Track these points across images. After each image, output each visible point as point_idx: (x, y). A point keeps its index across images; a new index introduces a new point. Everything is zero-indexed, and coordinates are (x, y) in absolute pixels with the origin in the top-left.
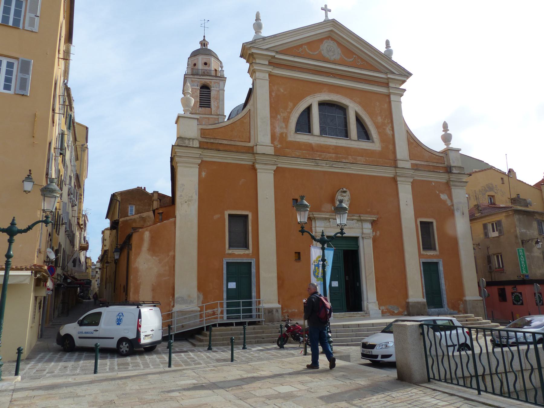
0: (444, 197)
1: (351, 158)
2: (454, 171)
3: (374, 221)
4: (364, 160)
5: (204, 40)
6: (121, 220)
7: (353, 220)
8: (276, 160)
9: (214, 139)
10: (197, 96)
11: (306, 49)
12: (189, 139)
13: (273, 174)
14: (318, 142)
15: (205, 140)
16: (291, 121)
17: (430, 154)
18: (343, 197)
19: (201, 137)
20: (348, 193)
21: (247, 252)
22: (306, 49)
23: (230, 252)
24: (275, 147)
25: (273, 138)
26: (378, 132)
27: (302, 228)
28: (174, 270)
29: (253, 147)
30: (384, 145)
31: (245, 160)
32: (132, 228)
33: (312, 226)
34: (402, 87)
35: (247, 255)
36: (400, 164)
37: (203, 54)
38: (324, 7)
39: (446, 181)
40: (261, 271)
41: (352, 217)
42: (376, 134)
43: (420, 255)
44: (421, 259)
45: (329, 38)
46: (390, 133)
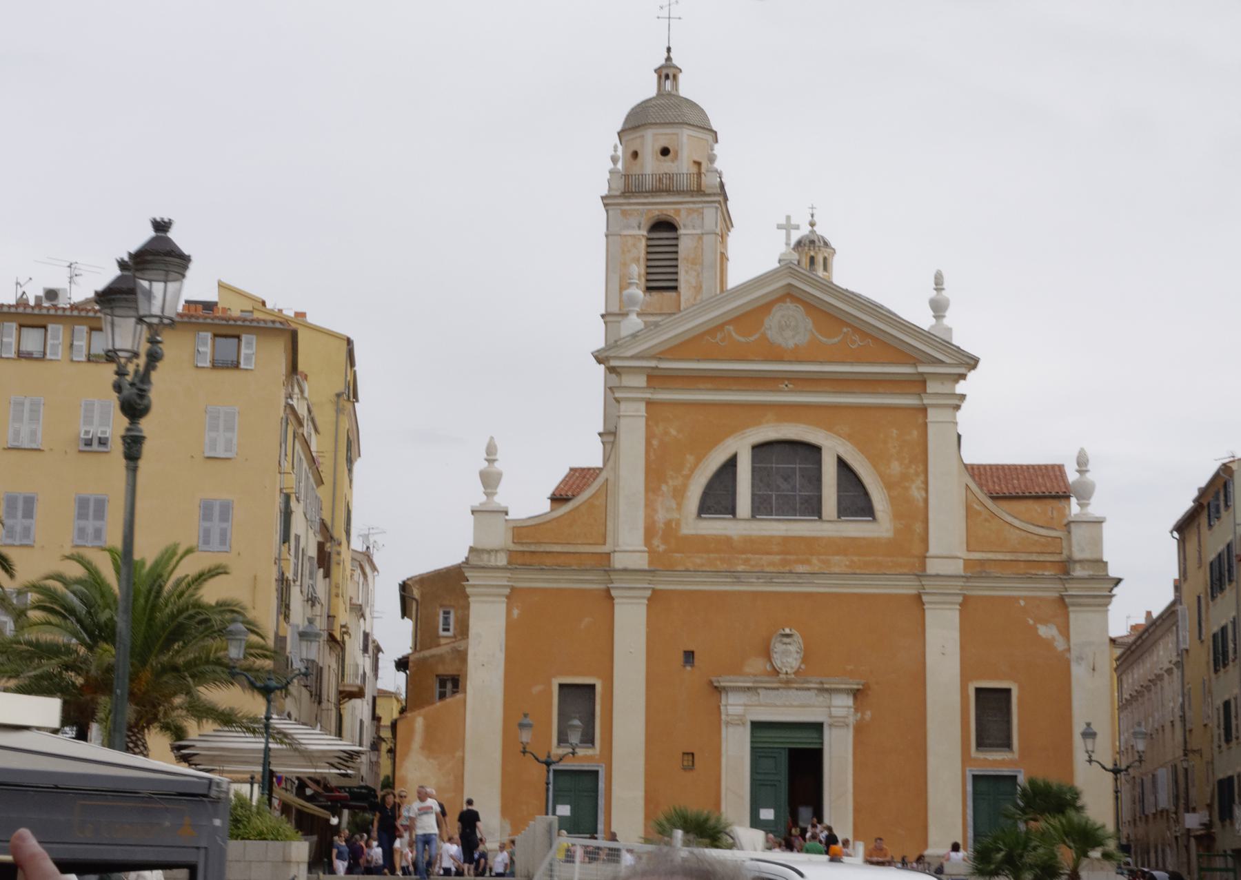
0: (1045, 631)
2: (1078, 572)
3: (858, 690)
4: (847, 563)
5: (669, 59)
6: (411, 658)
7: (809, 689)
8: (651, 578)
10: (639, 258)
12: (489, 552)
14: (745, 533)
16: (689, 494)
17: (1024, 534)
18: (784, 646)
19: (514, 542)
20: (798, 637)
24: (652, 552)
25: (649, 533)
26: (889, 496)
27: (524, 748)
28: (463, 782)
29: (609, 554)
31: (592, 583)
32: (437, 676)
33: (720, 702)
34: (960, 388)
35: (591, 758)
36: (933, 567)
37: (656, 124)
38: (783, 221)
39: (1057, 595)
40: (614, 787)
41: (803, 683)
43: (966, 759)
44: (968, 769)
45: (781, 299)
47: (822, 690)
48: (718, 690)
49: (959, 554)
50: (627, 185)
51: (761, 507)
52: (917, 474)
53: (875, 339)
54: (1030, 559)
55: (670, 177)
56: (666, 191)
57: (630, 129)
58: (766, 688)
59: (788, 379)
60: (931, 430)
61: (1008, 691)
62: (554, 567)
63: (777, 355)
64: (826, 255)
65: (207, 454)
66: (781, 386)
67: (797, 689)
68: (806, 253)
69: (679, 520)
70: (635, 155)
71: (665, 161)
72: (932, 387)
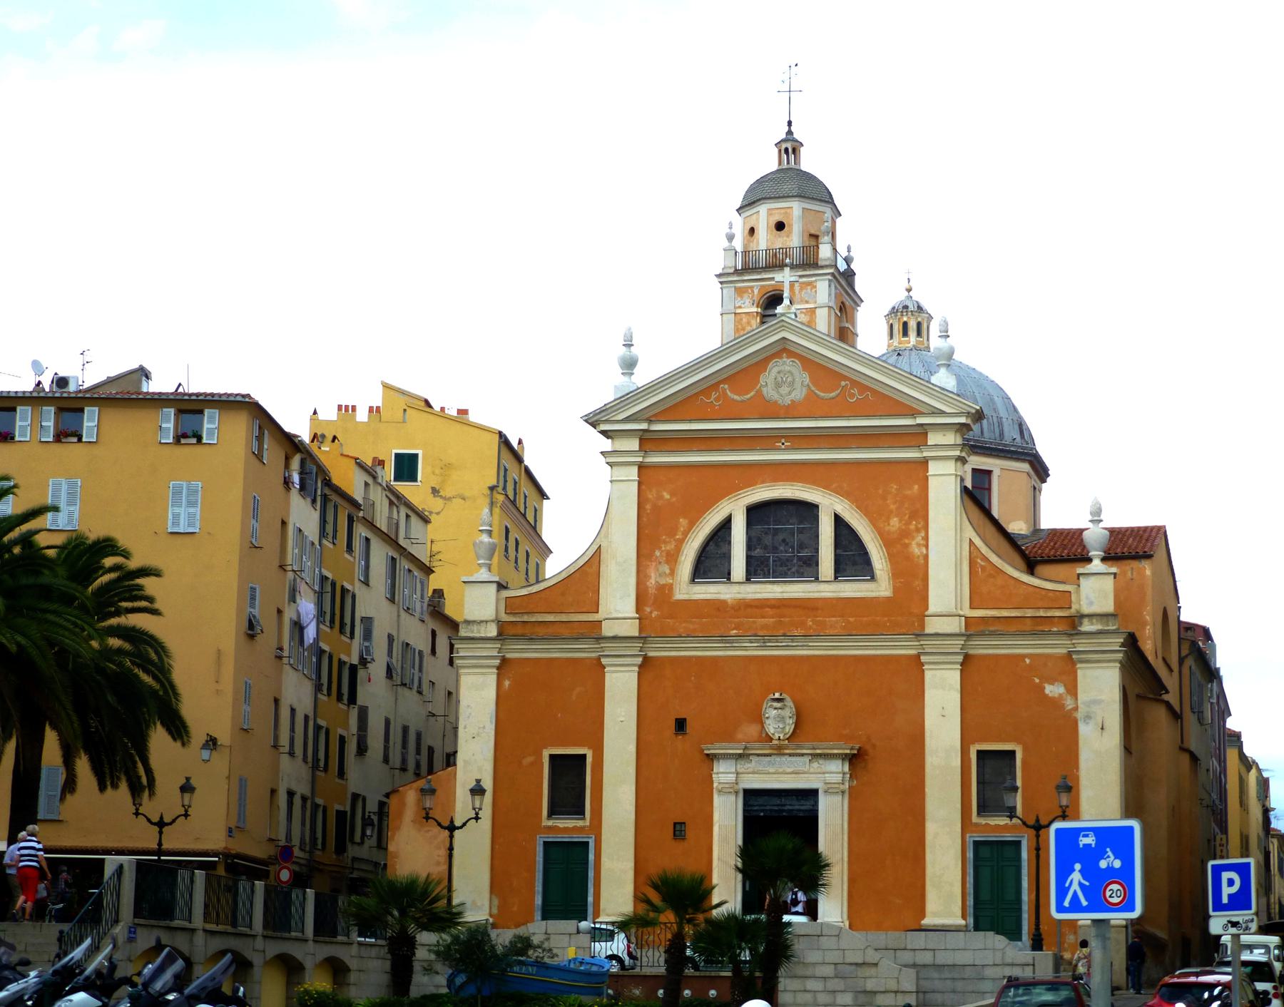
0: (1054, 690)
1: (811, 623)
2: (1087, 627)
3: (854, 755)
5: (790, 133)
7: (803, 755)
9: (530, 615)
11: (728, 391)
13: (636, 674)
14: (740, 596)
15: (514, 619)
16: (683, 558)
18: (776, 711)
19: (506, 613)
20: (789, 703)
21: (580, 823)
22: (728, 391)
23: (550, 823)
30: (900, 582)
33: (713, 770)
35: (581, 829)
36: (933, 626)
39: (1064, 651)
40: (604, 859)
42: (883, 560)
44: (968, 835)
45: (777, 355)
46: (919, 553)
47: (815, 756)
48: (711, 758)
49: (962, 613)
50: (745, 263)
51: (755, 569)
52: (918, 530)
53: (874, 392)
54: (1038, 615)
55: (786, 251)
56: (779, 266)
57: (746, 206)
58: (758, 755)
59: (783, 437)
60: (932, 483)
61: (1013, 753)
62: (545, 637)
63: (772, 411)
64: (919, 319)
65: (170, 530)
66: (777, 444)
67: (790, 755)
68: (899, 319)
69: (672, 584)
70: (752, 231)
71: (780, 236)
72: (933, 439)
